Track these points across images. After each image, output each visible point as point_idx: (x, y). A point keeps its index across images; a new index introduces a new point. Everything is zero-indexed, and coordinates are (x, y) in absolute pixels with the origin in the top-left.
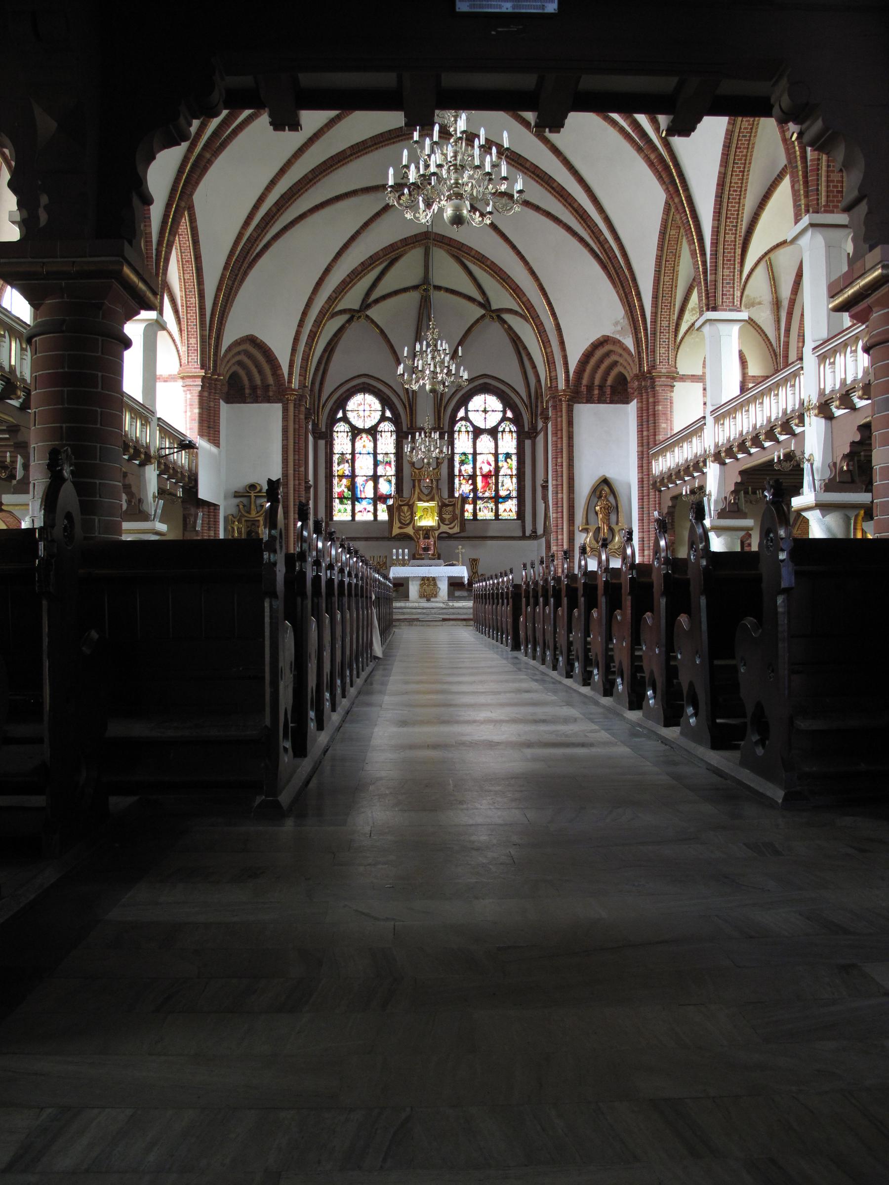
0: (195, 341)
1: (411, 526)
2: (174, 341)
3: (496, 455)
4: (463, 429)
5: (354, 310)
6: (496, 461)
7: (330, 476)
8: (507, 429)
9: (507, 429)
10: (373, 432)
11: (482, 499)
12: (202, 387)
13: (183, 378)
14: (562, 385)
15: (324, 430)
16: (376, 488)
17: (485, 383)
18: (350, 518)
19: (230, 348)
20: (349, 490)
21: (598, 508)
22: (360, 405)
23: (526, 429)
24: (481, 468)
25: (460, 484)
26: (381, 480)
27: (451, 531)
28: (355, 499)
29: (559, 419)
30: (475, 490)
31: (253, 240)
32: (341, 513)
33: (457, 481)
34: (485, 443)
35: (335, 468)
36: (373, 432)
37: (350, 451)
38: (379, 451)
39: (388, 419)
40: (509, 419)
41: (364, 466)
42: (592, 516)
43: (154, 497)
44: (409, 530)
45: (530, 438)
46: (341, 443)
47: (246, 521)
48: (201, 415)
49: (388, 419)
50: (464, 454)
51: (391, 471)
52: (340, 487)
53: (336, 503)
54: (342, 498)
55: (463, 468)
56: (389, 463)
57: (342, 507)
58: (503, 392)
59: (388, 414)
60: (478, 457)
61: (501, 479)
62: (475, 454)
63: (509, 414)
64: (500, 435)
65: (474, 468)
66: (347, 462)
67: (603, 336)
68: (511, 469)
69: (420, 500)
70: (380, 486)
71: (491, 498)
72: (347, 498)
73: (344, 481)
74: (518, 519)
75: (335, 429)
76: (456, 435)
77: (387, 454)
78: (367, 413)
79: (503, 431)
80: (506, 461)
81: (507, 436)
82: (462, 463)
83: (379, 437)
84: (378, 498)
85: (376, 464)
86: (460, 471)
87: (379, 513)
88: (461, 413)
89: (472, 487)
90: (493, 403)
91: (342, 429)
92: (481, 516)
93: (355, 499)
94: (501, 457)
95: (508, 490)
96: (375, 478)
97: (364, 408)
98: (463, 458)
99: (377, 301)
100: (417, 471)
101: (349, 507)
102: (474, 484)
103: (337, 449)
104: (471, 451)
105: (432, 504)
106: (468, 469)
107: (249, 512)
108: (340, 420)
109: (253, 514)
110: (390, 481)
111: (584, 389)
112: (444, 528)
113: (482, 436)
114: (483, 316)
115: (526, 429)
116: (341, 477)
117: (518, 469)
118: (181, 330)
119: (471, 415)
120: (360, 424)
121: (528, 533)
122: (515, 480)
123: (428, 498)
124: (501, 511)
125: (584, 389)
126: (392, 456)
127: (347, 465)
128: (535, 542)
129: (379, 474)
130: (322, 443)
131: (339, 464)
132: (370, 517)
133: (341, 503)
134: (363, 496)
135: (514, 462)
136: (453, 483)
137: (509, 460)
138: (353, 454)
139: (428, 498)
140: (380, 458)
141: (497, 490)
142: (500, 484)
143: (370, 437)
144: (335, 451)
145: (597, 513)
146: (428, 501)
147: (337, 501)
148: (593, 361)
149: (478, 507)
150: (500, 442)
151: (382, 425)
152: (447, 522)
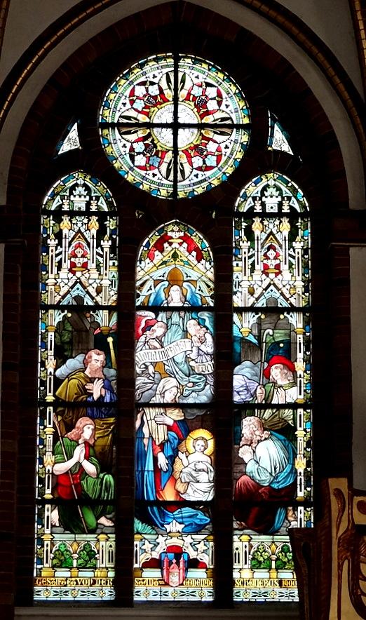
10: (214, 217)
16: (225, 461)
18: (107, 593)
20: (103, 467)
22: (156, 101)
26: (249, 426)
36: (214, 217)
37: (110, 297)
38: (238, 301)
41: (174, 356)
49: (278, 162)
51: (290, 387)
52: (68, 455)
53: (50, 530)
56: (283, 354)
57: (65, 539)
59: (279, 141)
66: (101, 345)
70: (245, 453)
73: (86, 429)
77: (273, 311)
78: (187, 138)
84: (236, 506)
85: (226, 355)
87: (242, 572)
96: (222, 417)
101: (105, 545)
103: (59, 284)
108: (72, 162)
110: (286, 433)
116: (72, 409)
120: (156, 182)
126: (296, 321)
127: (97, 358)
131: (61, 358)
132: (199, 586)
133: (71, 523)
134: (169, 495)
138: (126, 305)
140: (244, 325)
143: (198, 238)
144: (50, 298)
147: (53, 515)
151: (252, 189)
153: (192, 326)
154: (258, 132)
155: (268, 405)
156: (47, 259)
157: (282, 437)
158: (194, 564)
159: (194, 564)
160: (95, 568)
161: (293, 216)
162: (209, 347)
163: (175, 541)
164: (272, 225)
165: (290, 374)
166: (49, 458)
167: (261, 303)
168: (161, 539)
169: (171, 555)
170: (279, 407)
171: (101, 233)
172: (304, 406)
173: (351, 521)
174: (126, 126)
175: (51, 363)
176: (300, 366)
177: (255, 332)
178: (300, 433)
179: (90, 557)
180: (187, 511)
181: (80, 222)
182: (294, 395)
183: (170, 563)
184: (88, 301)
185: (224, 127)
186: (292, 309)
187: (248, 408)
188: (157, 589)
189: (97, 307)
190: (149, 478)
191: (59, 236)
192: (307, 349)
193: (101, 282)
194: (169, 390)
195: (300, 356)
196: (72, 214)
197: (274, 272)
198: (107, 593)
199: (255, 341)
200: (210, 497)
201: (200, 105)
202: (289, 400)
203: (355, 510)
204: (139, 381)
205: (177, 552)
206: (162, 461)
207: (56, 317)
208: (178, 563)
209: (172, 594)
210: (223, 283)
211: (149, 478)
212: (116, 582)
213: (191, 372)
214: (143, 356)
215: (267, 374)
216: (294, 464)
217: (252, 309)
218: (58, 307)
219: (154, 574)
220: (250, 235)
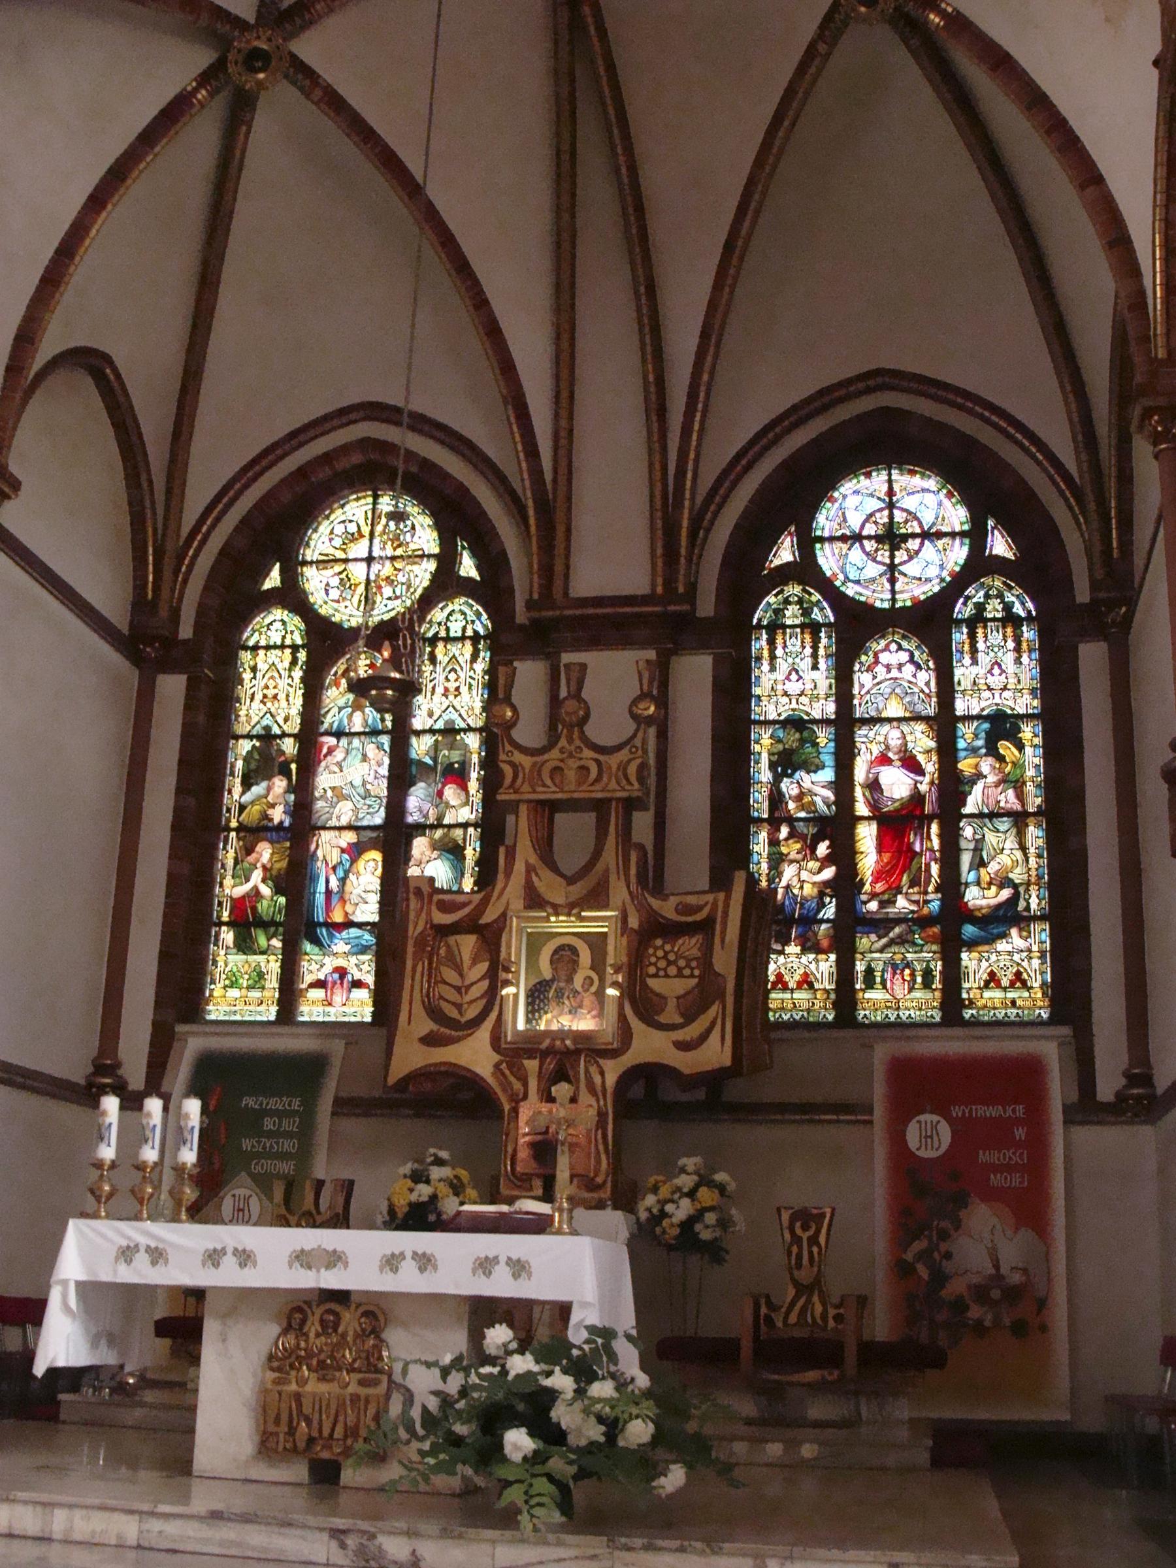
1: (484, 1033)
3: (944, 724)
4: (792, 616)
6: (947, 750)
8: (994, 609)
9: (994, 609)
11: (879, 925)
17: (886, 411)
20: (278, 890)
23: (1083, 595)
24: (874, 786)
25: (777, 861)
26: (420, 845)
28: (300, 926)
30: (846, 884)
33: (760, 844)
34: (893, 675)
35: (235, 793)
37: (294, 726)
38: (418, 723)
40: (998, 566)
41: (353, 777)
44: (476, 1055)
45: (1099, 631)
46: (268, 691)
49: (466, 587)
50: (797, 723)
51: (463, 807)
54: (246, 921)
55: (788, 787)
56: (456, 774)
57: (237, 960)
58: (969, 442)
59: (468, 567)
60: (861, 734)
61: (968, 832)
62: (846, 723)
63: (1000, 546)
64: (960, 636)
65: (843, 784)
66: (285, 771)
68: (1019, 786)
69: (534, 900)
71: (923, 922)
72: (266, 925)
73: (265, 852)
74: (1053, 1020)
76: (760, 644)
77: (450, 731)
79: (978, 619)
81: (993, 638)
82: (786, 763)
85: (402, 774)
86: (776, 799)
88: (785, 553)
89: (829, 873)
90: (927, 499)
92: (874, 1002)
93: (300, 926)
94: (966, 733)
95: (1004, 882)
98: (792, 738)
100: (526, 761)
101: (273, 966)
102: (844, 856)
103: (251, 714)
104: (831, 708)
105: (598, 922)
106: (816, 785)
110: (454, 851)
112: (651, 1045)
115: (1083, 595)
116: (253, 833)
117: (1052, 784)
119: (827, 559)
121: (1106, 1091)
122: (1035, 835)
123: (578, 890)
124: (970, 987)
126: (473, 741)
127: (280, 784)
128: (1146, 1132)
131: (247, 784)
133: (244, 945)
134: (338, 917)
137: (1006, 748)
139: (578, 890)
140: (420, 748)
141: (951, 886)
142: (966, 859)
144: (242, 728)
146: (573, 907)
147: (228, 936)
149: (860, 967)
150: (963, 673)
151: (438, 614)
152: (671, 1015)
153: (371, 750)
154: (446, 561)
155: (439, 825)
156: (244, 691)
157: (451, 857)
158: (358, 984)
159: (358, 984)
160: (263, 988)
161: (476, 638)
162: (384, 771)
163: (341, 962)
164: (454, 649)
165: (463, 794)
166: (229, 881)
167: (440, 725)
168: (327, 960)
169: (336, 976)
170: (450, 826)
171: (294, 662)
172: (476, 826)
173: (429, 920)
174: (324, 563)
175: (237, 789)
176: (473, 785)
177: (432, 753)
178: (469, 853)
180: (354, 932)
181: (274, 655)
182: (466, 814)
183: (334, 983)
184: (276, 730)
186: (470, 729)
187: (420, 828)
188: (321, 1009)
189: (284, 735)
190: (320, 899)
191: (254, 669)
192: (481, 768)
193: (288, 710)
194: (344, 813)
195: (474, 775)
196: (268, 648)
199: (430, 762)
200: (375, 918)
202: (461, 820)
203: (434, 908)
204: (320, 804)
205: (342, 972)
206: (334, 884)
207: (245, 746)
208: (342, 984)
209: (334, 1014)
211: (320, 899)
212: (280, 1002)
213: (367, 795)
214: (324, 780)
215: (440, 794)
216: (460, 884)
217: (432, 731)
218: (249, 736)
219: (317, 994)
220: (433, 659)
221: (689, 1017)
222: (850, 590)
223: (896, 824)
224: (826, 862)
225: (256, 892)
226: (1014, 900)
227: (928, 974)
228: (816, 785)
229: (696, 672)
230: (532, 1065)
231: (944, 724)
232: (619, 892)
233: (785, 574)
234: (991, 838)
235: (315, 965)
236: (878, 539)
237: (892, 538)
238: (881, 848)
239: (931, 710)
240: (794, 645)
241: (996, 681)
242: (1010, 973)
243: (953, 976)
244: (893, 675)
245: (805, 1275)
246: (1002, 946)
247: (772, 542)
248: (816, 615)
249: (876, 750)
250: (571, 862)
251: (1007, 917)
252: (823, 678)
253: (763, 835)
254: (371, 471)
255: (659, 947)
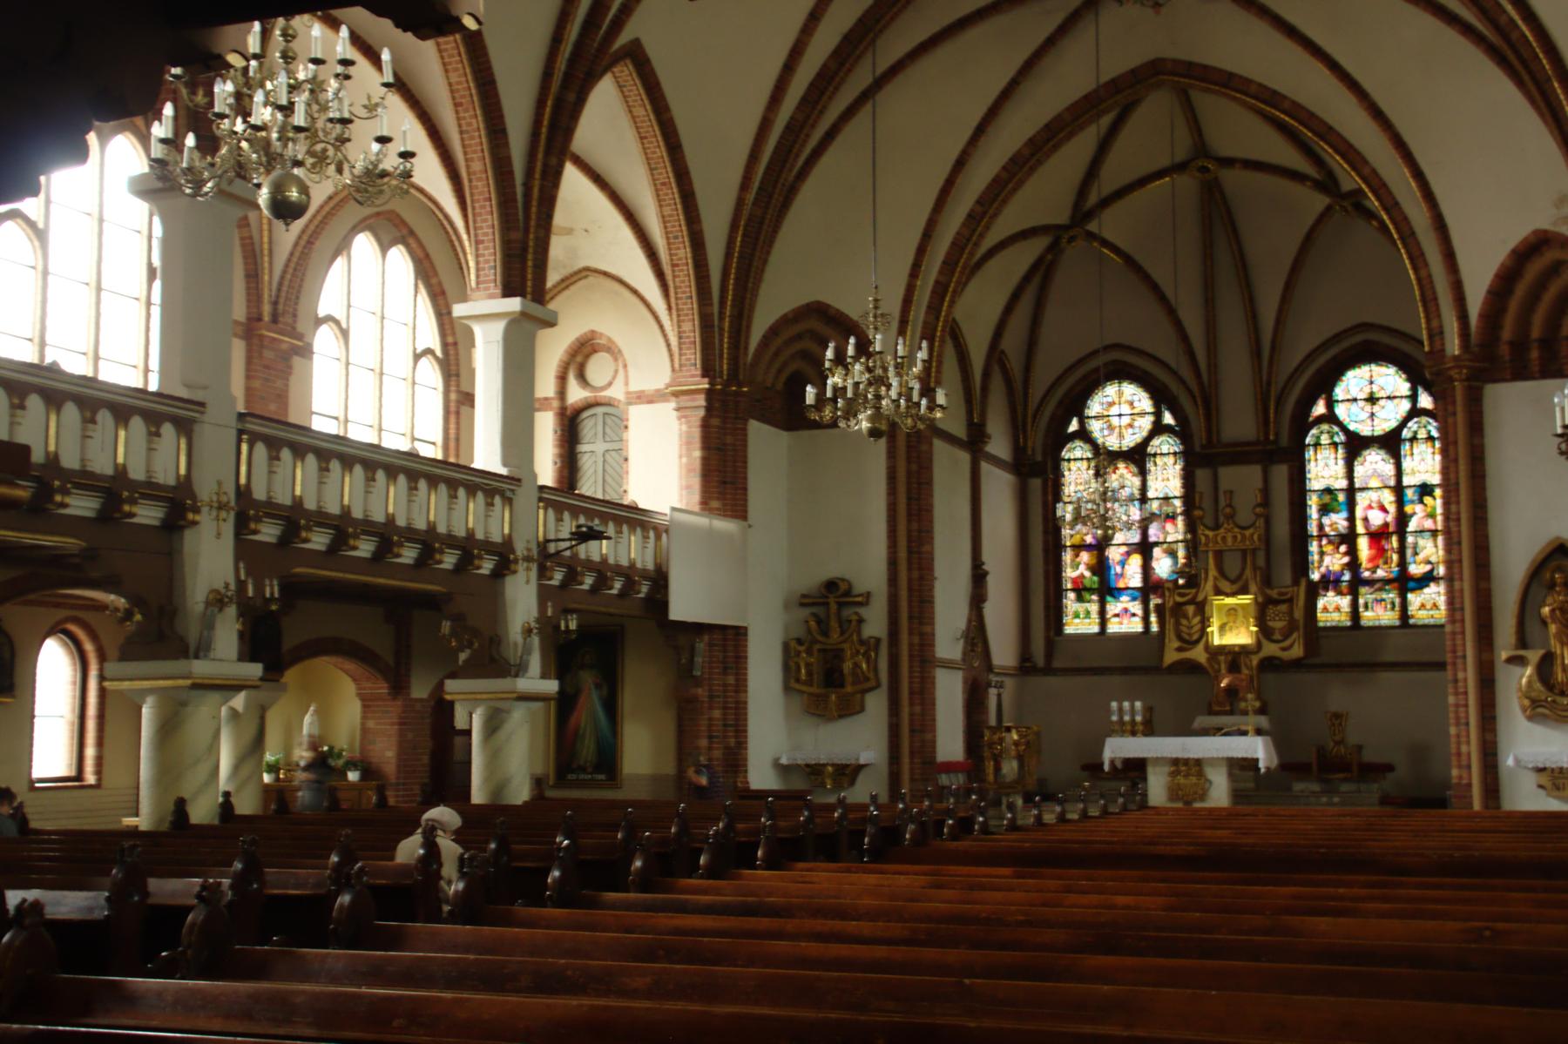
0: (692, 328)
1: (1201, 646)
2: (661, 327)
3: (1399, 490)
4: (1325, 439)
5: (1058, 227)
7: (1054, 548)
8: (1422, 434)
9: (1422, 434)
10: (1138, 457)
11: (1369, 583)
12: (709, 409)
13: (676, 394)
14: (1453, 346)
15: (1039, 458)
16: (1147, 568)
18: (1095, 629)
19: (773, 331)
20: (1094, 573)
21: (1546, 610)
24: (1366, 520)
26: (1157, 551)
27: (1286, 655)
28: (1106, 589)
29: (1450, 420)
31: (796, 130)
32: (1080, 620)
33: (1314, 547)
34: (1374, 464)
35: (1066, 532)
36: (1138, 457)
38: (1150, 494)
39: (1168, 429)
42: (1533, 629)
43: (528, 631)
44: (1198, 654)
47: (823, 651)
48: (706, 464)
49: (1168, 429)
50: (1328, 491)
51: (1176, 532)
52: (1076, 568)
53: (1070, 602)
54: (1081, 590)
55: (1326, 521)
56: (1171, 518)
59: (1168, 419)
61: (1410, 539)
62: (1351, 491)
64: (1406, 448)
65: (1351, 519)
67: (1536, 232)
69: (1218, 592)
70: (1154, 564)
72: (1091, 590)
75: (1065, 454)
76: (1309, 454)
77: (1166, 499)
79: (1414, 439)
80: (1421, 502)
81: (1422, 449)
82: (1325, 510)
83: (1150, 466)
84: (1151, 586)
86: (1321, 527)
88: (1320, 409)
89: (1346, 559)
90: (1390, 379)
91: (1078, 454)
95: (1429, 562)
96: (1145, 548)
97: (1121, 410)
98: (1327, 499)
99: (1105, 203)
100: (1211, 534)
101: (1094, 608)
102: (1353, 552)
104: (1343, 484)
105: (1245, 599)
106: (1338, 520)
107: (826, 633)
109: (835, 635)
110: (1172, 554)
111: (1504, 350)
112: (1270, 649)
113: (1366, 453)
114: (1329, 208)
116: (1079, 548)
118: (670, 308)
119: (1340, 411)
120: (1113, 443)
122: (1440, 539)
123: (1235, 587)
125: (1504, 350)
126: (1178, 503)
129: (1152, 539)
130: (1036, 483)
133: (1080, 599)
134: (1121, 585)
135: (1436, 502)
136: (1306, 553)
137: (1427, 500)
139: (1235, 587)
141: (1403, 564)
142: (1409, 552)
143: (1134, 469)
145: (1544, 623)
146: (1233, 594)
147: (1071, 595)
148: (1521, 290)
149: (1361, 601)
150: (1407, 464)
151: (1156, 442)
152: (1277, 636)
154: (1158, 415)
158: (1134, 615)
159: (1134, 615)
164: (1165, 459)
179: (1088, 614)
181: (1079, 464)
185: (1143, 414)
197: (1167, 479)
198: (1095, 629)
201: (1131, 404)
205: (1126, 610)
210: (1144, 488)
211: (1113, 577)
219: (1116, 620)
221: (1286, 637)
222: (1352, 427)
223: (1378, 536)
224: (1346, 554)
225: (1082, 576)
226: (1432, 571)
227: (1393, 604)
228: (1338, 520)
229: (1281, 473)
230: (1222, 658)
231: (1399, 490)
232: (1253, 587)
233: (1320, 420)
234: (1421, 542)
235: (1113, 607)
236: (1366, 400)
237: (1372, 399)
238: (1371, 547)
239: (1392, 483)
240: (1326, 454)
241: (1422, 467)
242: (1429, 604)
243: (1404, 605)
244: (1374, 464)
245: (1337, 738)
246: (1426, 590)
247: (1313, 402)
248: (1336, 439)
249: (1366, 503)
250: (1233, 574)
251: (1428, 579)
252: (1340, 469)
253: (1315, 543)
254: (1121, 373)
255: (1271, 610)
